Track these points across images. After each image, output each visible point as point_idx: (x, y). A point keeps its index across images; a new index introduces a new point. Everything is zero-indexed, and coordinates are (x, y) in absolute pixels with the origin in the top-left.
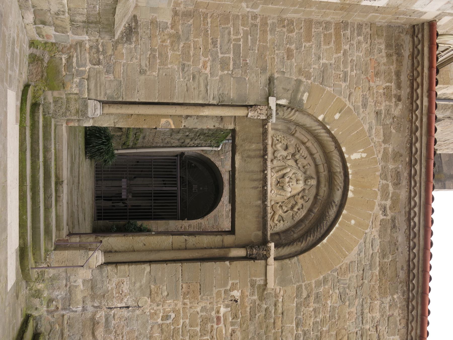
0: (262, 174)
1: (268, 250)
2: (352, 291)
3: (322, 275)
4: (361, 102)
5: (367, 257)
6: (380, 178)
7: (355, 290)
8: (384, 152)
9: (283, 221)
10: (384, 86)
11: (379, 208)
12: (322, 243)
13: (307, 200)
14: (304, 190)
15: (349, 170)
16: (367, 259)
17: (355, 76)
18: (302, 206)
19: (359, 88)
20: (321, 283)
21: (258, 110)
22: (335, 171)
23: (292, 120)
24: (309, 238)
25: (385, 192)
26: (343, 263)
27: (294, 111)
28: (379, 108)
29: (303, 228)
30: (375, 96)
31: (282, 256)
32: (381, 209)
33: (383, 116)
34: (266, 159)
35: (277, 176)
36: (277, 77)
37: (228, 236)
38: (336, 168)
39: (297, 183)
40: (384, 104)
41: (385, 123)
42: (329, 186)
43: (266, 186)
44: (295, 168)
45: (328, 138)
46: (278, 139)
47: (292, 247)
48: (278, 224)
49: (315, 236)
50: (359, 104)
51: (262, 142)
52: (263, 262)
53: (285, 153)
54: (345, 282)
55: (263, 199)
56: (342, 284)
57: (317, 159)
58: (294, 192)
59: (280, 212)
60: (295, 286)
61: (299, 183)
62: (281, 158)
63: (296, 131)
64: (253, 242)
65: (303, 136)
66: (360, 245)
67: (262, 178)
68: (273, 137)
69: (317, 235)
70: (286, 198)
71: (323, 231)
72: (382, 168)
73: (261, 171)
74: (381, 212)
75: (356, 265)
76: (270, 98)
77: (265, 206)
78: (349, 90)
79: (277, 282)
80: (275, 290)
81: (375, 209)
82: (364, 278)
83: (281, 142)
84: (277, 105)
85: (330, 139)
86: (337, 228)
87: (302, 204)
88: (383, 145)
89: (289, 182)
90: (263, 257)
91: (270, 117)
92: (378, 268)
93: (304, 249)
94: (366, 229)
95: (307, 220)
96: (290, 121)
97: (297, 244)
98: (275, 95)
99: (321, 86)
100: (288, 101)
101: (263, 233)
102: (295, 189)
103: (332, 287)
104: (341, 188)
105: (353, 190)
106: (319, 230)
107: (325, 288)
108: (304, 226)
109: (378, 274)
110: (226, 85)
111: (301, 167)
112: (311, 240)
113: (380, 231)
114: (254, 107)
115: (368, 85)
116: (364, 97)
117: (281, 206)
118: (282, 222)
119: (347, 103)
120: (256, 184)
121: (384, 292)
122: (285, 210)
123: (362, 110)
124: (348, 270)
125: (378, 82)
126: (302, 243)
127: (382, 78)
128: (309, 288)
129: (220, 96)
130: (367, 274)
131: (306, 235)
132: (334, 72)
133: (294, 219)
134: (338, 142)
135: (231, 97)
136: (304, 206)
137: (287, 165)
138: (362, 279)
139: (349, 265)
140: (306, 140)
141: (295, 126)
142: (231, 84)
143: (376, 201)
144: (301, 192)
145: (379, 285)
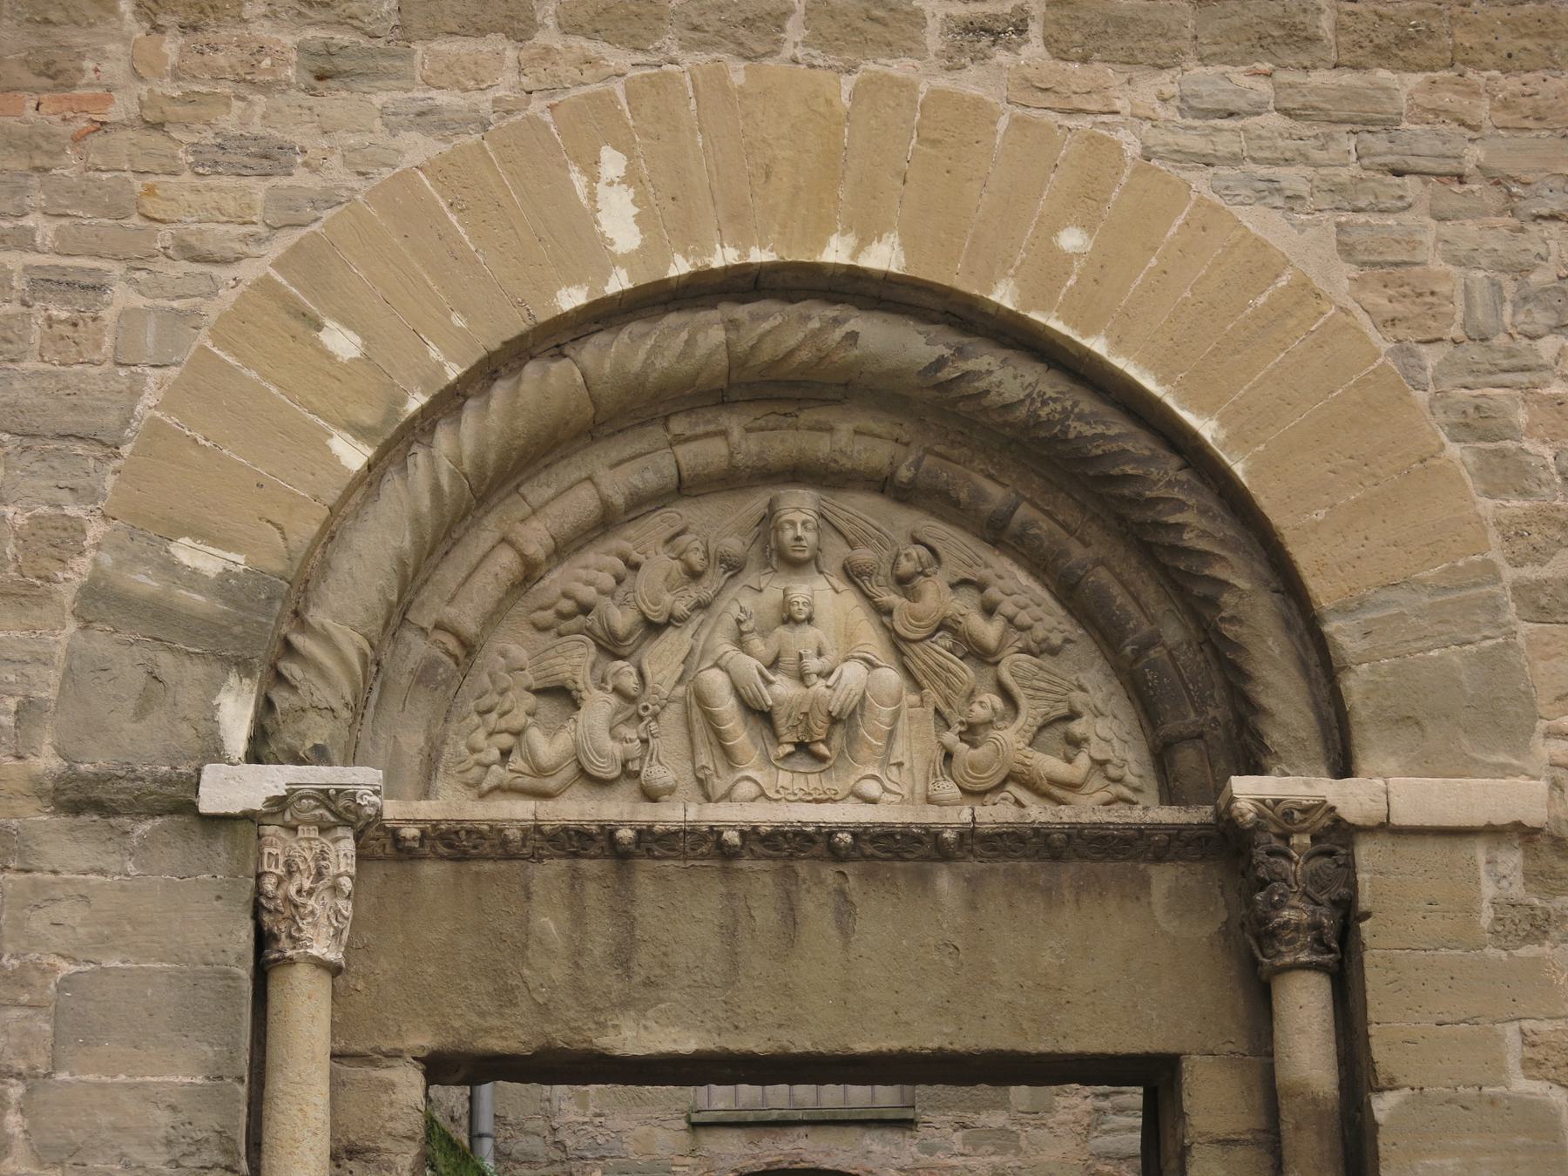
0: (744, 864)
1: (1284, 816)
2: (1543, 252)
3: (1442, 446)
4: (244, 181)
5: (1309, 147)
7: (1532, 228)
8: (594, 34)
9: (1073, 716)
10: (136, 29)
11: (974, 70)
12: (1224, 446)
14: (853, 575)
15: (717, 262)
16: (1323, 148)
17: (65, 222)
18: (963, 590)
19: (150, 191)
20: (1495, 452)
21: (293, 890)
22: (721, 359)
23: (363, 656)
24: (1189, 539)
25: (867, 25)
26: (1351, 305)
27: (299, 640)
28: (287, 63)
29: (1118, 577)
30: (204, 89)
31: (1322, 720)
32: (981, 57)
33: (343, 38)
34: (639, 832)
35: (756, 757)
36: (61, 753)
37: (1187, 1103)
38: (702, 349)
39: (809, 620)
40: (263, 31)
41: (394, 20)
42: (825, 402)
43: (831, 834)
44: (703, 637)
45: (494, 404)
46: (495, 754)
48: (1097, 750)
49: (1177, 493)
50: (260, 196)
51: (516, 864)
52: (1367, 854)
53: (598, 708)
54: (1481, 295)
55: (927, 858)
56: (1498, 314)
57: (636, 481)
58: (871, 640)
59: (1010, 738)
60: (1524, 628)
61: (809, 604)
62: (630, 733)
63: (439, 626)
64: (1226, 923)
65: (480, 579)
66: (1225, 190)
67: (780, 864)
68: (485, 786)
69: (1169, 484)
70: (915, 698)
71: (1140, 444)
72: (702, 45)
73: (725, 872)
74: (1001, 56)
75: (1361, 218)
76: (207, 805)
78: (160, 264)
81: (977, 92)
82: (1450, 166)
83: (518, 734)
84: (255, 756)
85: (500, 390)
86: (1117, 343)
87: (953, 586)
88: (540, 38)
89: (802, 677)
90: (1330, 854)
91: (342, 803)
92: (1383, 75)
93: (1263, 571)
94: (1121, 151)
95: (1065, 554)
96: (374, 665)
97: (1233, 619)
98: (183, 769)
99: (126, 450)
100: (233, 680)
101: (1158, 859)
102: (849, 637)
103: (1523, 378)
104: (836, 322)
105: (851, 240)
106: (1129, 470)
107: (1530, 427)
108: (1103, 575)
109: (1420, 77)
110: (104, 1119)
111: (696, 592)
112: (1204, 523)
113: (1130, 61)
114: (266, 918)
115: (130, 133)
116: (209, 161)
117: (971, 733)
118: (1077, 728)
119: (248, 272)
120: (815, 907)
121: (1542, 34)
122: (998, 702)
123: (301, 178)
124: (1401, 271)
125: (106, 67)
126: (1224, 585)
127: (78, 38)
128: (1536, 538)
129: (188, 1162)
130: (1423, 148)
132: (30, 364)
133: (1056, 639)
134: (522, 338)
135: (199, 1080)
136: (964, 574)
137: (681, 690)
138: (1461, 178)
139: (1363, 264)
140: (506, 559)
141: (409, 636)
142: (102, 1086)
143: (923, 88)
144: (867, 597)
145: (1497, 67)
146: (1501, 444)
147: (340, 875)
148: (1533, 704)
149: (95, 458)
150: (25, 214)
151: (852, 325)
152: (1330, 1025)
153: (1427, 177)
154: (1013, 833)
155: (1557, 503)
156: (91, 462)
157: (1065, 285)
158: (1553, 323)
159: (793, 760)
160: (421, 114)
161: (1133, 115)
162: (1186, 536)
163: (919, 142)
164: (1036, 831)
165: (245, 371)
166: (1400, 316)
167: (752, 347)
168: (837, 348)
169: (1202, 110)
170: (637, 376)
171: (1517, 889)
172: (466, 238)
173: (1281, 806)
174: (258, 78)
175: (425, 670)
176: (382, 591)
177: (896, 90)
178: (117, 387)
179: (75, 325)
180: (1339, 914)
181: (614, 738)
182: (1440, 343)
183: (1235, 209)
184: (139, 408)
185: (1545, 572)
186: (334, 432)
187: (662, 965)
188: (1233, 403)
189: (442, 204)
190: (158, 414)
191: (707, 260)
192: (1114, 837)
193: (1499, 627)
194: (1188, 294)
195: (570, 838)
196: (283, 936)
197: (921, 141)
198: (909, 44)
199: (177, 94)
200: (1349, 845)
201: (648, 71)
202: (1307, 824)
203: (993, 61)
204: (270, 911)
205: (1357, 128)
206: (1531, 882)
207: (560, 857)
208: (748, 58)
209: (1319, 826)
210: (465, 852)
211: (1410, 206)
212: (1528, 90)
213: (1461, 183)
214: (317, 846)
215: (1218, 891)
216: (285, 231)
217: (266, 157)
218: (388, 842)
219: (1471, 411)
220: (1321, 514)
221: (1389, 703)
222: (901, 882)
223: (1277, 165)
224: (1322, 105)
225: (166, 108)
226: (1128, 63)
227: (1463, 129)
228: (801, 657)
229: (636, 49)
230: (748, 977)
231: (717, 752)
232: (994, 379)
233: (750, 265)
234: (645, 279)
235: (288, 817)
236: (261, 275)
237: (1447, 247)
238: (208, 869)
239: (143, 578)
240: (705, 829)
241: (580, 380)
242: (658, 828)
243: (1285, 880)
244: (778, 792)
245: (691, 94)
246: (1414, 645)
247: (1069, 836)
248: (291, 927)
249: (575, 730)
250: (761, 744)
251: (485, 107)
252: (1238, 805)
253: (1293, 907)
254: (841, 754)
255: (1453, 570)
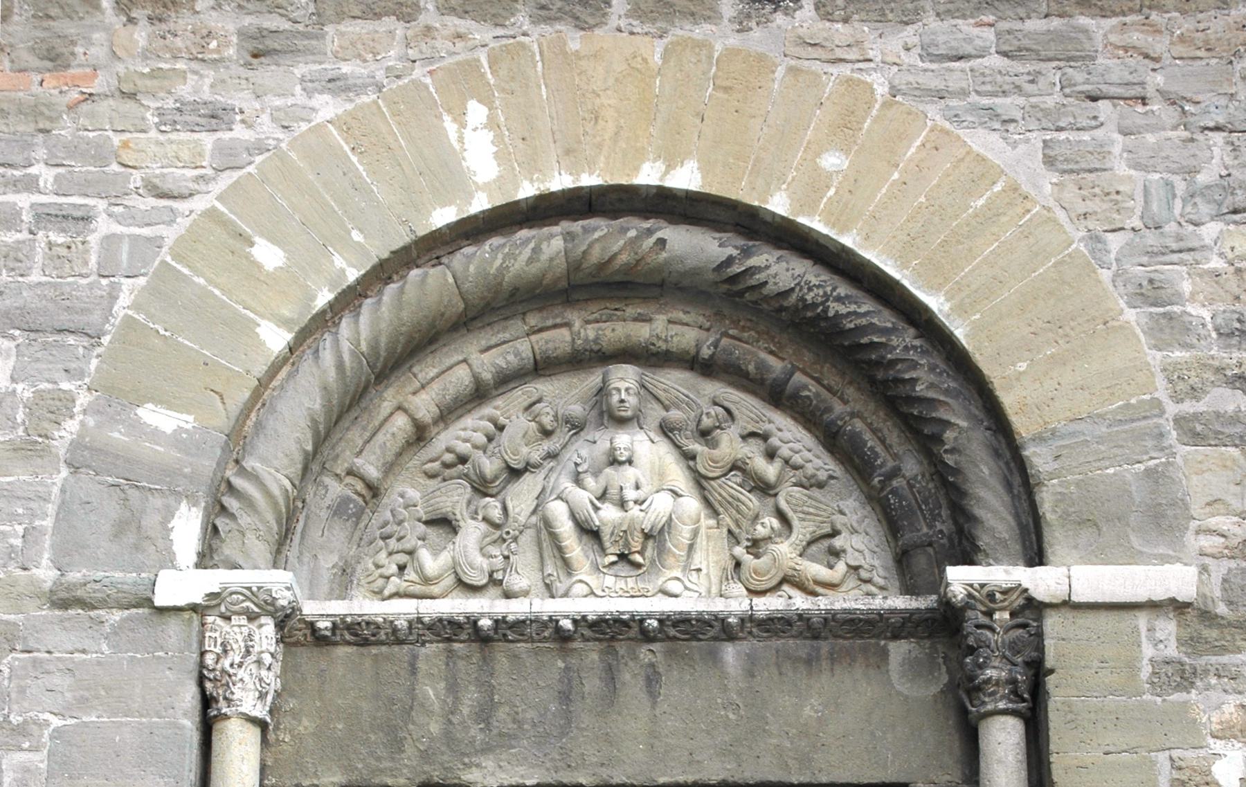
0: (576, 645)
3: (1121, 312)
4: (196, 136)
6: (597, 31)
10: (116, 21)
13: (720, 410)
16: (1032, 82)
17: (61, 170)
19: (125, 145)
22: (561, 265)
27: (238, 482)
28: (228, 45)
31: (1022, 528)
32: (764, 22)
39: (630, 462)
40: (214, 21)
43: (642, 621)
47: (972, 477)
50: (209, 146)
52: (1053, 624)
54: (1158, 194)
55: (715, 639)
56: (1170, 208)
62: (495, 551)
66: (956, 118)
67: (605, 644)
72: (549, 20)
73: (562, 649)
74: (779, 18)
75: (1063, 136)
77: (749, 620)
79: (1161, 550)
80: (1207, 560)
88: (423, 19)
89: (622, 504)
90: (1024, 626)
92: (1083, 21)
94: (872, 91)
97: (952, 451)
99: (106, 340)
104: (650, 232)
105: (660, 166)
107: (1192, 294)
109: (1114, 21)
113: (882, 18)
115: (111, 102)
116: (168, 121)
119: (199, 204)
120: (632, 678)
123: (240, 132)
126: (947, 424)
130: (1114, 78)
131: (905, 409)
134: (406, 249)
138: (1144, 100)
143: (718, 47)
146: (1168, 308)
147: (262, 652)
148: (1187, 509)
149: (85, 347)
150: (31, 165)
151: (659, 234)
152: (1022, 757)
153: (1115, 101)
154: (782, 618)
155: (1212, 352)
156: (81, 350)
157: (825, 195)
158: (1214, 213)
159: (616, 567)
160: (330, 81)
161: (883, 62)
162: (918, 389)
163: (713, 89)
164: (800, 616)
165: (196, 279)
166: (1090, 210)
167: (584, 252)
168: (650, 252)
169: (938, 55)
170: (495, 277)
171: (1172, 651)
172: (364, 174)
173: (986, 589)
174: (207, 56)
175: (339, 505)
176: (298, 441)
177: (697, 50)
178: (99, 293)
179: (69, 247)
180: (1031, 673)
181: (484, 555)
182: (1122, 232)
183: (960, 132)
184: (116, 308)
185: (1201, 407)
186: (264, 323)
187: (514, 721)
188: (957, 282)
189: (347, 148)
190: (130, 312)
191: (547, 185)
192: (860, 620)
193: (1162, 450)
194: (922, 199)
195: (444, 627)
196: (221, 698)
197: (716, 87)
198: (708, 13)
199: (147, 70)
200: (1039, 619)
201: (505, 41)
202: (1006, 603)
203: (774, 25)
204: (210, 680)
205: (1062, 64)
206: (1183, 645)
207: (438, 642)
208: (583, 29)
209: (1016, 604)
210: (366, 639)
211: (1102, 124)
212: (1201, 26)
213: (1144, 104)
214: (245, 630)
215: (941, 660)
216: (228, 172)
217: (213, 117)
218: (308, 632)
219: (1145, 283)
220: (1022, 366)
221: (1073, 509)
222: (697, 657)
223: (996, 96)
224: (1034, 47)
225: (139, 83)
226: (881, 21)
227: (1147, 61)
228: (621, 488)
229: (496, 25)
230: (577, 728)
231: (559, 563)
232: (772, 271)
233: (580, 189)
234: (500, 201)
235: (223, 609)
236: (209, 206)
237: (1131, 156)
238: (162, 648)
239: (116, 435)
240: (545, 618)
241: (451, 280)
242: (510, 618)
243: (988, 647)
244: (603, 591)
245: (538, 58)
246: (1094, 464)
247: (825, 619)
248: (226, 691)
249: (454, 550)
250: (592, 556)
251: (380, 75)
252: (952, 588)
253: (994, 667)
254: (653, 562)
255: (1128, 406)
